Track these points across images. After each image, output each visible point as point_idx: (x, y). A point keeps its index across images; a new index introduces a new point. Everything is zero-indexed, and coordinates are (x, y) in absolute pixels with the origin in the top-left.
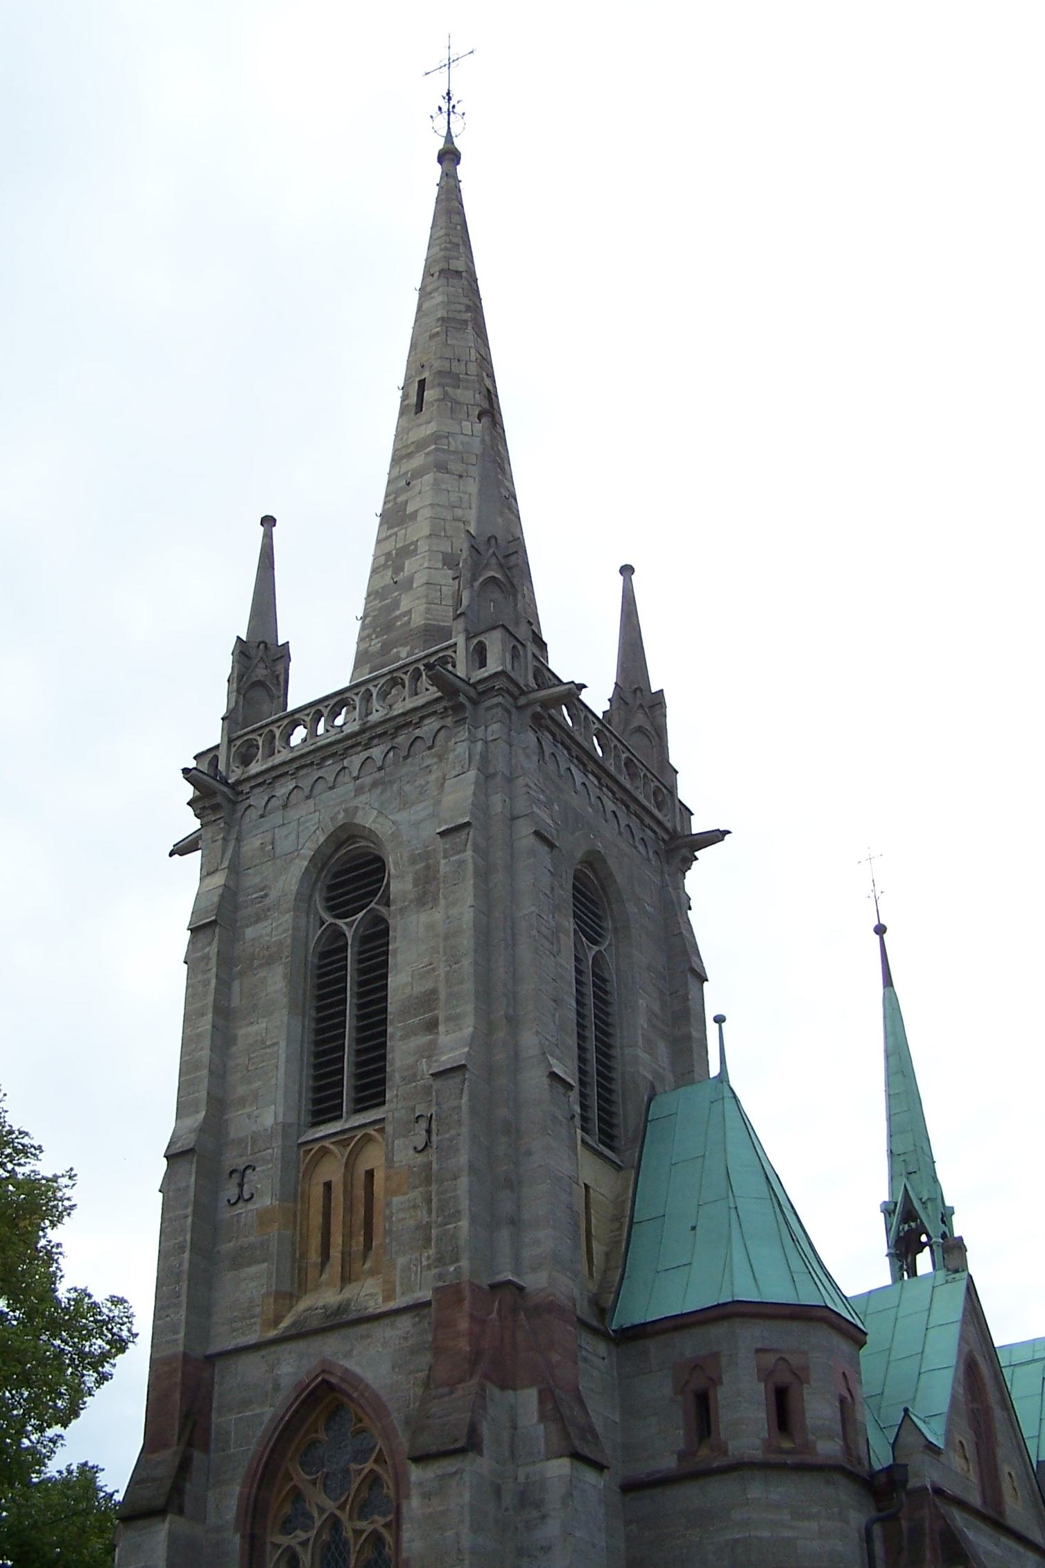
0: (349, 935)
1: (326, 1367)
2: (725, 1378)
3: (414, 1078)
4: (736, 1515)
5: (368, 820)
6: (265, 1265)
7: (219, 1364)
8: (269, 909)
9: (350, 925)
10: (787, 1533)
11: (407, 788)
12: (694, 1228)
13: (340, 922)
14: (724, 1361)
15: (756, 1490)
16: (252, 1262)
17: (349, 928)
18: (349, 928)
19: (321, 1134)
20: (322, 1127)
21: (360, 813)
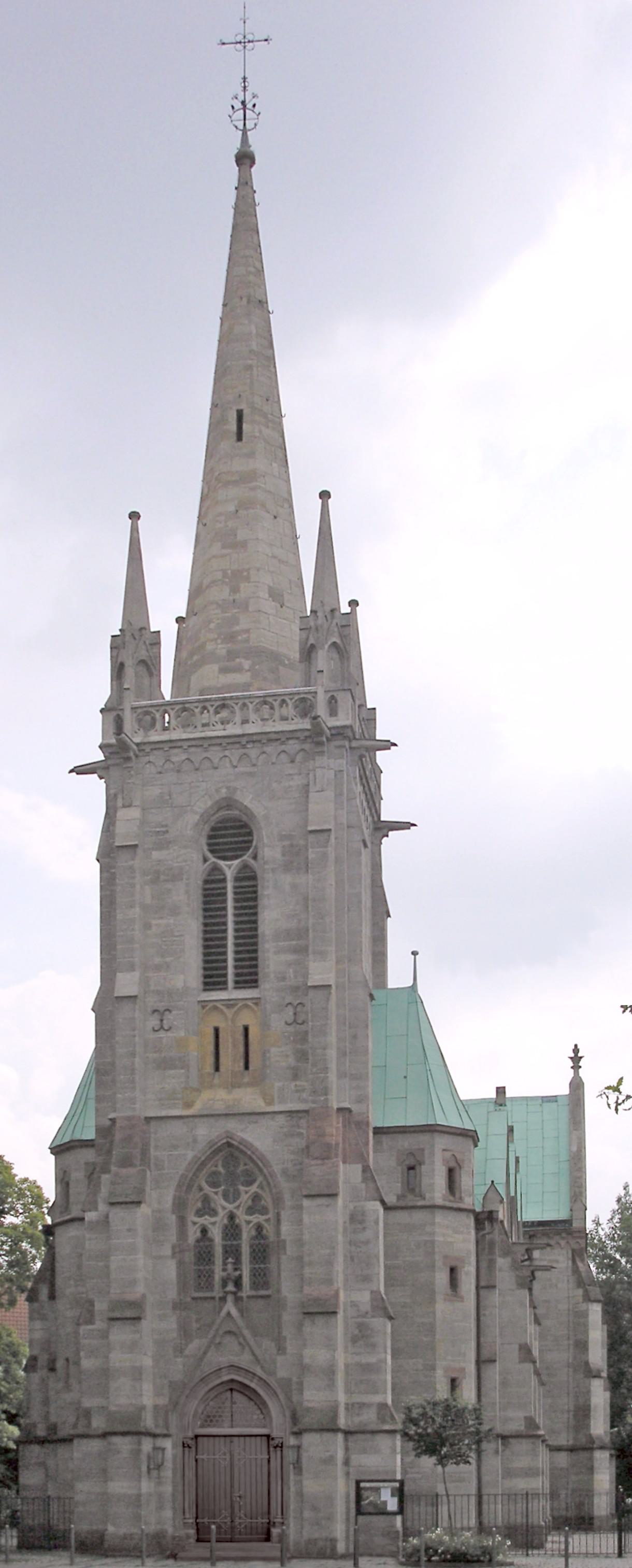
0: (230, 874)
1: (229, 1135)
2: (427, 1162)
3: (284, 979)
4: (428, 1229)
5: (247, 800)
6: (183, 1071)
7: (153, 1123)
8: (170, 842)
9: (230, 867)
10: (450, 1240)
11: (275, 785)
12: (405, 1077)
13: (222, 863)
14: (426, 1152)
15: (440, 1218)
16: (175, 1068)
17: (230, 868)
18: (230, 868)
19: (214, 998)
20: (213, 993)
21: (239, 792)
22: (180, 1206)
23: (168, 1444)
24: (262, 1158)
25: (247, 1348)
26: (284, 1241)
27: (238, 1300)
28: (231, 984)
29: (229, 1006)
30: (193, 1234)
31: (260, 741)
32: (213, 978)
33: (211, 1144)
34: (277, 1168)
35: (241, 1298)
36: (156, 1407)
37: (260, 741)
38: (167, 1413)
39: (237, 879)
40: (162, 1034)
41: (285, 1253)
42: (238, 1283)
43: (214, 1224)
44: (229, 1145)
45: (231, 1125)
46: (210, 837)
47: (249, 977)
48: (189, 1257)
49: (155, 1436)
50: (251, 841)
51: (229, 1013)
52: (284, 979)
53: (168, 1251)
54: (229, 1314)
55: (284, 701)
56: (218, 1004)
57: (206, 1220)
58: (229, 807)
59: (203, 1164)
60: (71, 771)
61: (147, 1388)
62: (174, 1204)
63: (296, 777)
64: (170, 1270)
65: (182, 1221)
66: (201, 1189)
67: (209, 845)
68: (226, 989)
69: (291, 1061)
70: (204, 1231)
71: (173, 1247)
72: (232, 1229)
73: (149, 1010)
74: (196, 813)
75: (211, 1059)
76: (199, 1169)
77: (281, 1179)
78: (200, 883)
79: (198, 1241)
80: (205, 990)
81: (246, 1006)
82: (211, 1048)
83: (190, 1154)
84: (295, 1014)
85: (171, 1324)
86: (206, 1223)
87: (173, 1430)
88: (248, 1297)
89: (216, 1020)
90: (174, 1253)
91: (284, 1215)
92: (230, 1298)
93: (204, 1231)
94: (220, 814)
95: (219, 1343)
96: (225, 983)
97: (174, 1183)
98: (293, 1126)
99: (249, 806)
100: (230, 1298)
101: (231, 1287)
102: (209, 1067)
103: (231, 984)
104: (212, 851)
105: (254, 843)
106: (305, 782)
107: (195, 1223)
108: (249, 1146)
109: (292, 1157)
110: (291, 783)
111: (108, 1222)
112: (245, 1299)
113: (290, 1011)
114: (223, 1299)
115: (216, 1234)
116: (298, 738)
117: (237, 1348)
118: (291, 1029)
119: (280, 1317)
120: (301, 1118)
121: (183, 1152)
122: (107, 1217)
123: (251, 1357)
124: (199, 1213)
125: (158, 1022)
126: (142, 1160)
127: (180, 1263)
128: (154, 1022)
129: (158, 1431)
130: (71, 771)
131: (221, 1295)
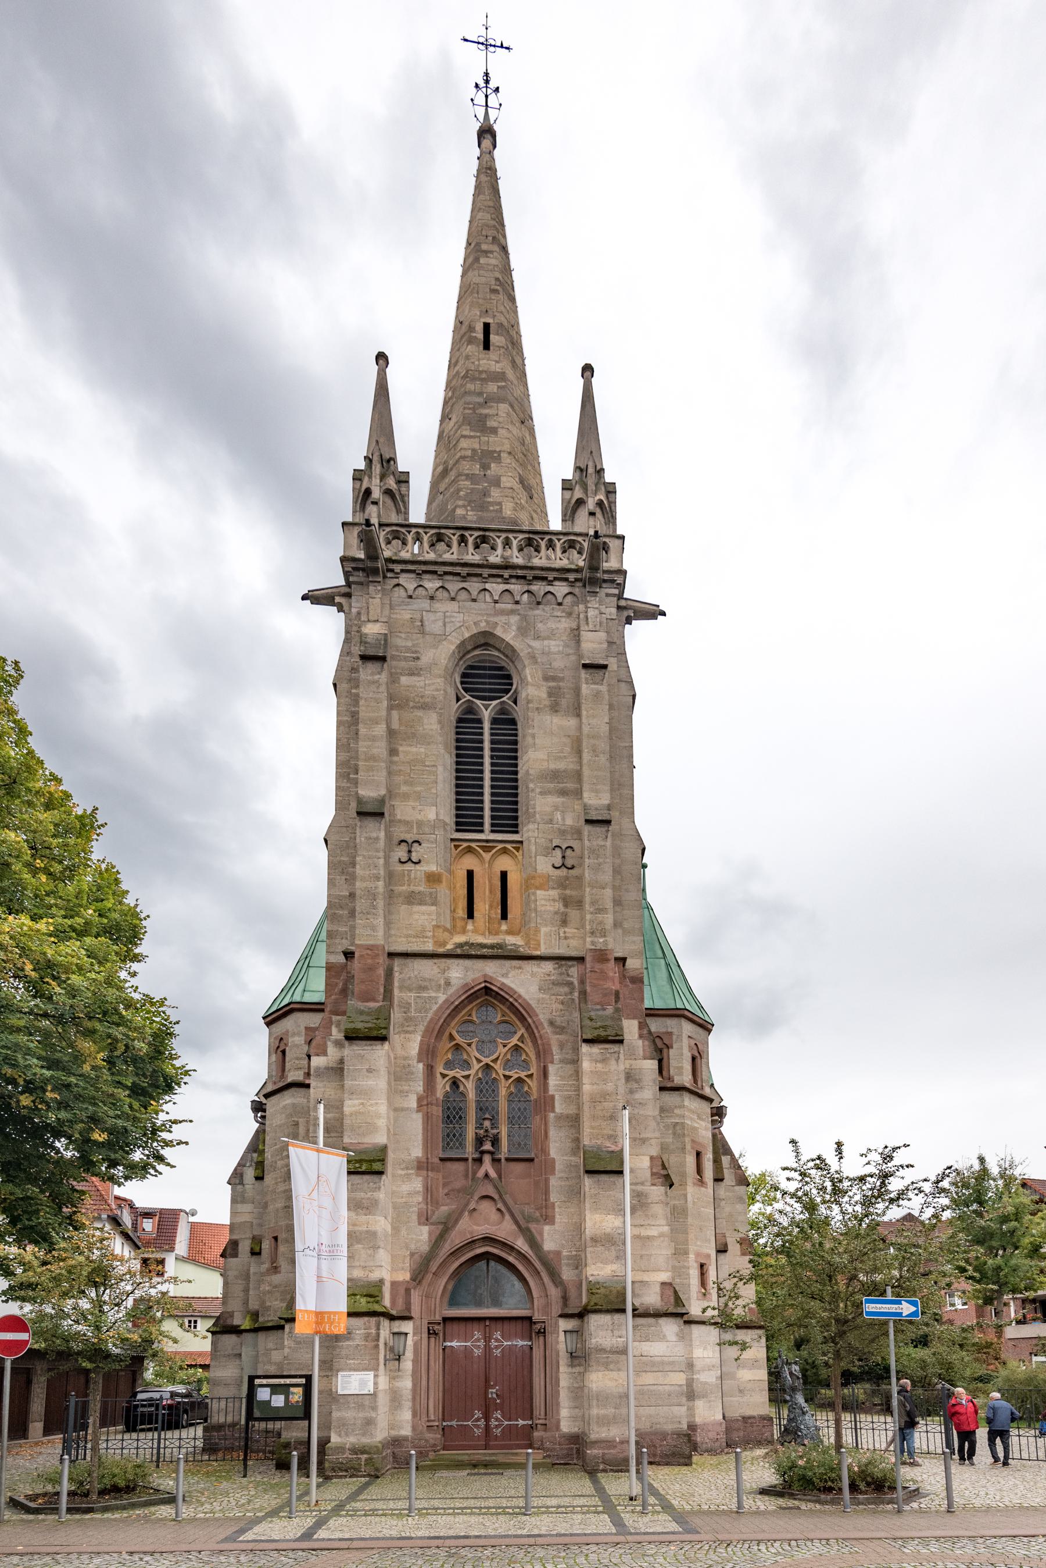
9: (486, 707)
13: (478, 702)
22: (428, 1054)
23: (407, 1327)
24: (527, 1007)
25: (507, 1217)
26: (553, 1097)
27: (496, 1161)
28: (487, 826)
29: (486, 849)
30: (442, 1087)
31: (524, 577)
32: (466, 818)
33: (467, 988)
34: (543, 1017)
35: (499, 1160)
36: (393, 1284)
37: (524, 577)
38: (408, 1291)
39: (494, 721)
40: (409, 866)
41: (553, 1111)
42: (495, 1141)
43: (467, 1077)
44: (487, 990)
45: (491, 969)
46: (464, 675)
47: (508, 819)
48: (437, 1111)
49: (392, 1318)
50: (511, 684)
51: (487, 856)
52: (551, 821)
53: (414, 1105)
54: (487, 1175)
55: (550, 540)
56: (473, 845)
57: (459, 1073)
58: (486, 645)
59: (457, 1009)
60: (304, 598)
61: (383, 1256)
62: (420, 1049)
63: (563, 620)
64: (415, 1124)
65: (430, 1069)
66: (451, 1038)
67: (462, 683)
68: (482, 831)
69: (559, 906)
70: (455, 1083)
71: (420, 1100)
72: (487, 1084)
73: (396, 841)
74: (452, 643)
75: (463, 903)
76: (452, 1015)
77: (548, 1030)
78: (453, 719)
79: (447, 1095)
80: (457, 831)
81: (505, 851)
82: (464, 892)
83: (442, 998)
84: (564, 857)
85: (417, 1184)
86: (458, 1075)
87: (415, 1312)
88: (507, 1160)
89: (469, 862)
90: (420, 1106)
91: (552, 1069)
92: (487, 1158)
93: (455, 1083)
94: (477, 652)
95: (474, 1209)
96: (482, 824)
97: (422, 1028)
98: (561, 974)
99: (511, 642)
100: (487, 1158)
101: (487, 1146)
102: (462, 912)
103: (487, 826)
104: (465, 689)
105: (514, 687)
106: (574, 625)
107: (444, 1076)
108: (512, 992)
109: (561, 1007)
110: (558, 625)
111: (342, 1070)
112: (503, 1160)
113: (558, 853)
114: (479, 1161)
115: (470, 1088)
116: (566, 580)
117: (494, 1216)
118: (558, 872)
119: (547, 1181)
120: (570, 967)
121: (434, 995)
122: (341, 1061)
123: (514, 1227)
124: (449, 1065)
125: (406, 855)
126: (384, 997)
127: (427, 1119)
128: (401, 853)
129: (394, 1312)
130: (304, 598)
131: (477, 1156)
